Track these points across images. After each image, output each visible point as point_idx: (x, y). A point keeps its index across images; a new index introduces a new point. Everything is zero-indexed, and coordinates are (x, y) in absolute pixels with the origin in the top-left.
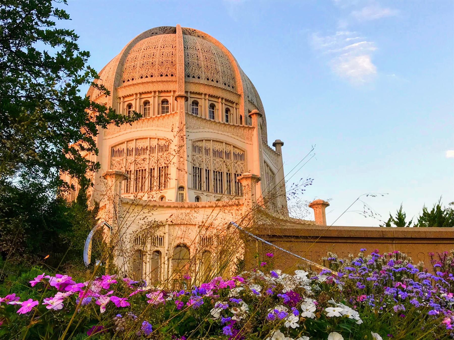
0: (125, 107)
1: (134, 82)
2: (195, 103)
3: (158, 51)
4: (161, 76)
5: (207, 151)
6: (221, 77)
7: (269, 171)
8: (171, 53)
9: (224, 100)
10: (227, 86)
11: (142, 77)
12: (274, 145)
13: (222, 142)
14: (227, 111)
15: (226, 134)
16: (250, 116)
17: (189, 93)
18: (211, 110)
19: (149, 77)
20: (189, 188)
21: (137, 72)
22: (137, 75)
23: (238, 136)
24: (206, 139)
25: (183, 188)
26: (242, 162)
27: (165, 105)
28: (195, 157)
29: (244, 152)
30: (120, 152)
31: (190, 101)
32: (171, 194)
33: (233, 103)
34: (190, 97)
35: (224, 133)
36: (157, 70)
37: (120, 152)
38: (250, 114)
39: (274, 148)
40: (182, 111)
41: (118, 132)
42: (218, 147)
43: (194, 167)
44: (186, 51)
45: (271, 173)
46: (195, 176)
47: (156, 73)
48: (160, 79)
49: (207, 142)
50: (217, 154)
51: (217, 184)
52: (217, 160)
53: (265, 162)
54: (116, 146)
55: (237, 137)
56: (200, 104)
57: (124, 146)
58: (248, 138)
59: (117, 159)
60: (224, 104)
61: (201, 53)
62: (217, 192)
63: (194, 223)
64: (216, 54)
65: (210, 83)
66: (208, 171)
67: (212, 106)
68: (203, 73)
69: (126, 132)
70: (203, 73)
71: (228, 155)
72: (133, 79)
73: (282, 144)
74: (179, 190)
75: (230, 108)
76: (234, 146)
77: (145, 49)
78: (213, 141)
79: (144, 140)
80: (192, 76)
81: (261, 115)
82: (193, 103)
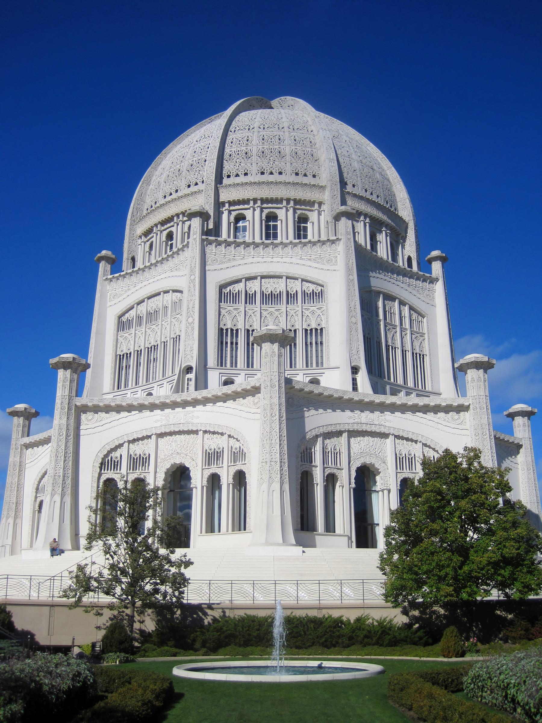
1: (158, 205)
4: (189, 186)
11: (165, 197)
15: (288, 260)
22: (161, 195)
23: (310, 260)
24: (247, 276)
26: (319, 305)
29: (323, 286)
33: (311, 203)
35: (285, 260)
47: (182, 184)
48: (188, 191)
54: (123, 314)
57: (132, 313)
58: (329, 261)
63: (195, 429)
68: (254, 164)
69: (136, 288)
70: (254, 164)
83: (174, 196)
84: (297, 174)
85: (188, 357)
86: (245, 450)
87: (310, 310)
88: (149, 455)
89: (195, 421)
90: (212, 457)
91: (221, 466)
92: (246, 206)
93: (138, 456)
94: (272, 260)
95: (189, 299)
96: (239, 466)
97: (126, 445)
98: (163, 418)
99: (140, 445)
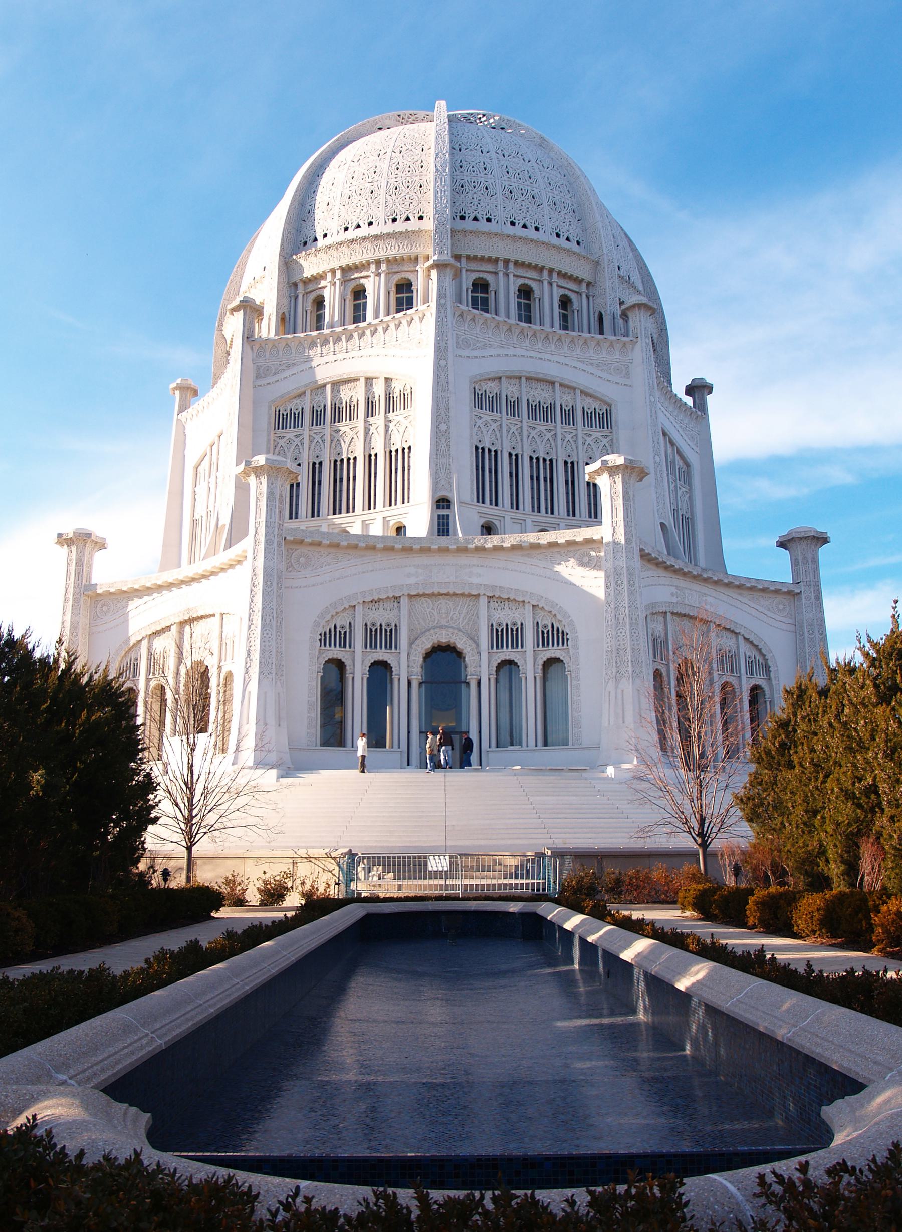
0: (309, 306)
2: (481, 286)
3: (387, 162)
5: (513, 407)
6: (547, 218)
7: (677, 458)
8: (419, 164)
9: (555, 275)
10: (562, 240)
11: (346, 229)
12: (689, 391)
13: (553, 383)
14: (565, 302)
16: (624, 315)
17: (463, 260)
18: (523, 301)
19: (364, 226)
20: (461, 502)
21: (336, 218)
24: (508, 374)
25: (448, 501)
27: (405, 295)
28: (479, 422)
29: (610, 406)
30: (296, 419)
31: (467, 281)
32: (418, 520)
33: (578, 281)
34: (467, 270)
36: (382, 207)
37: (296, 419)
38: (623, 307)
39: (689, 401)
40: (443, 301)
41: (288, 367)
42: (541, 395)
43: (477, 448)
44: (456, 158)
45: (681, 463)
46: (479, 469)
48: (390, 228)
49: (513, 381)
50: (542, 412)
51: (538, 489)
52: (539, 428)
53: (665, 434)
55: (590, 369)
56: (491, 288)
59: (290, 433)
60: (554, 285)
61: (495, 161)
62: (539, 511)
63: (474, 592)
64: (533, 161)
65: (518, 231)
66: (515, 460)
67: (525, 292)
71: (568, 416)
72: (325, 236)
73: (709, 389)
74: (438, 507)
75: (573, 296)
76: (582, 392)
77: (356, 160)
78: (528, 379)
79: (351, 385)
80: (472, 218)
81: (653, 309)
82: (474, 285)
83: (365, 231)
84: (558, 236)
85: (443, 482)
86: (566, 630)
87: (592, 438)
89: (475, 580)
92: (490, 267)
94: (540, 356)
95: (440, 396)
96: (553, 652)
97: (359, 609)
98: (420, 571)
99: (381, 610)
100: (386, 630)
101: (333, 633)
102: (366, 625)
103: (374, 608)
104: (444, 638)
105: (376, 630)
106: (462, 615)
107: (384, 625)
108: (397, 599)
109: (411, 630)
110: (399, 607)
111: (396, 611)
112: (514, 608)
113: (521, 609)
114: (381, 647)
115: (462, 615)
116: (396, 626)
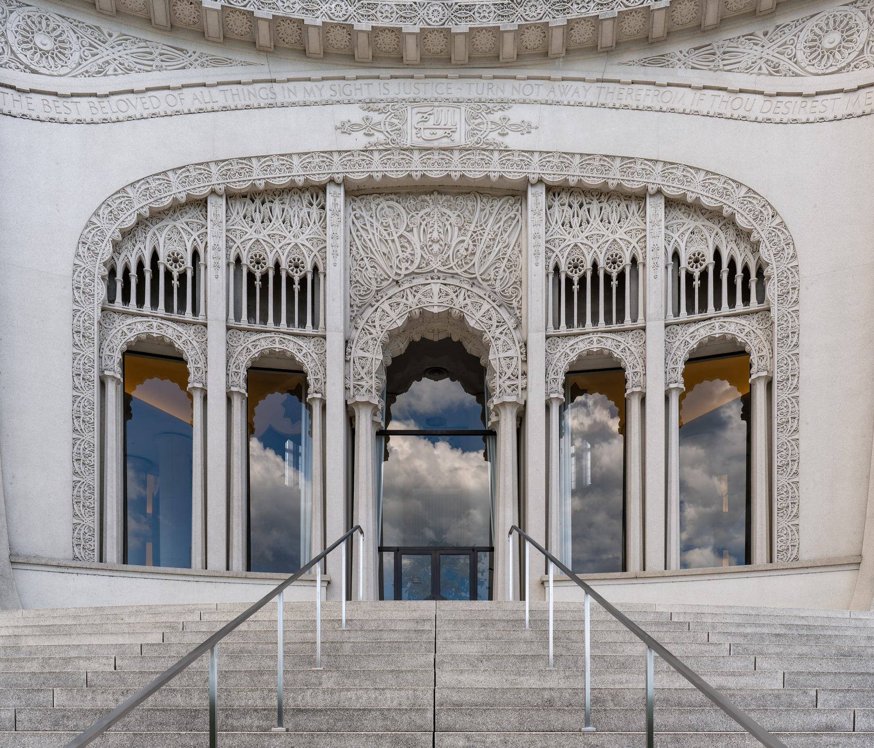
88: (315, 269)
90: (594, 291)
91: (640, 323)
93: (270, 264)
100: (290, 280)
101: (148, 277)
102: (238, 260)
103: (258, 217)
104: (435, 299)
105: (265, 277)
106: (481, 247)
107: (284, 265)
108: (317, 191)
109: (352, 282)
110: (323, 219)
111: (317, 227)
112: (614, 218)
113: (634, 219)
114: (277, 320)
115: (481, 247)
116: (315, 269)
